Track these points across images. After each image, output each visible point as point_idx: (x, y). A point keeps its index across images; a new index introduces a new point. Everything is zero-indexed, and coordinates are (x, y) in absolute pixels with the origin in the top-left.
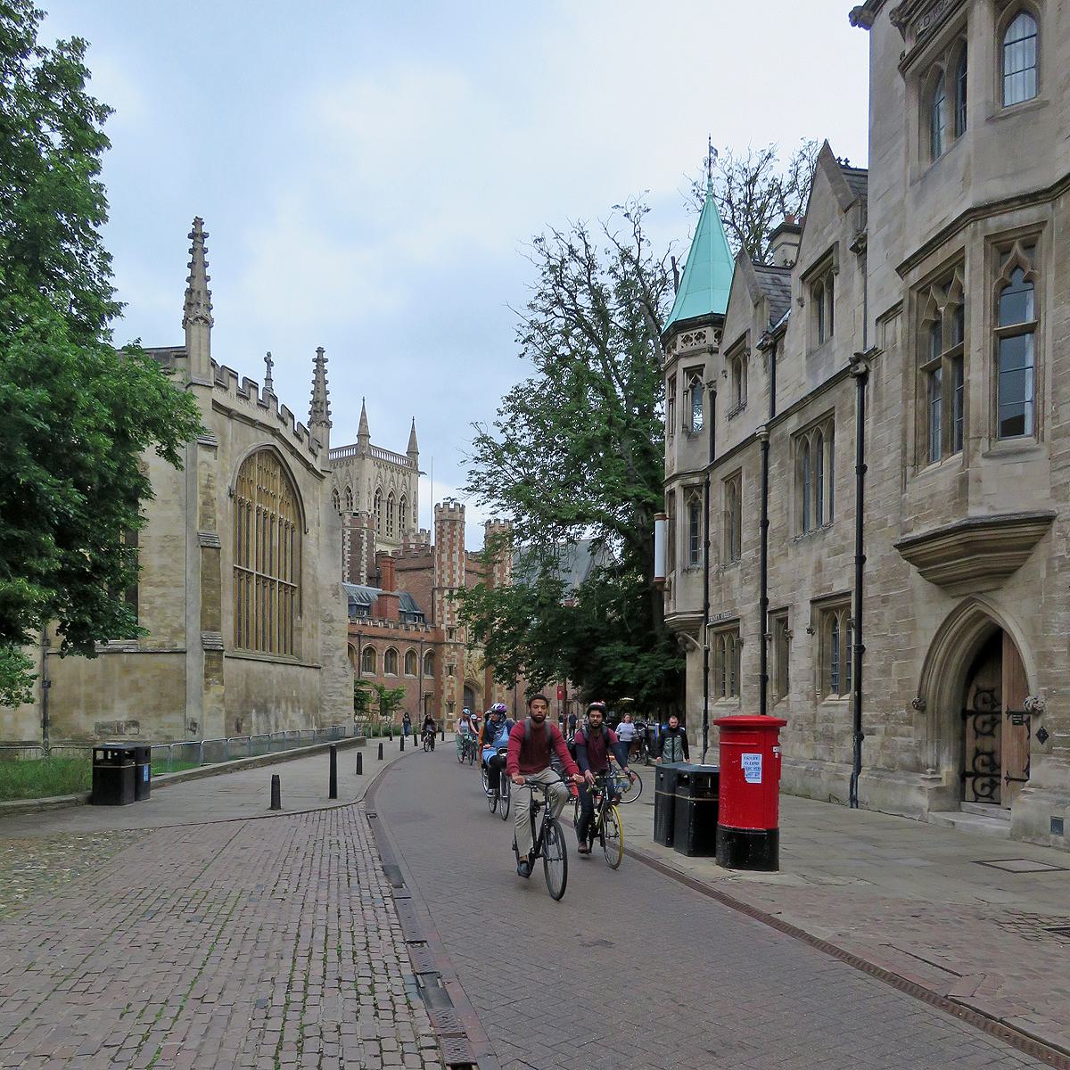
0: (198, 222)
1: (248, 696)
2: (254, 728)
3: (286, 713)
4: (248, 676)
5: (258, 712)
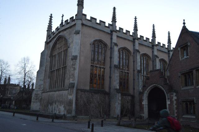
2: (49, 109)
5: (50, 105)
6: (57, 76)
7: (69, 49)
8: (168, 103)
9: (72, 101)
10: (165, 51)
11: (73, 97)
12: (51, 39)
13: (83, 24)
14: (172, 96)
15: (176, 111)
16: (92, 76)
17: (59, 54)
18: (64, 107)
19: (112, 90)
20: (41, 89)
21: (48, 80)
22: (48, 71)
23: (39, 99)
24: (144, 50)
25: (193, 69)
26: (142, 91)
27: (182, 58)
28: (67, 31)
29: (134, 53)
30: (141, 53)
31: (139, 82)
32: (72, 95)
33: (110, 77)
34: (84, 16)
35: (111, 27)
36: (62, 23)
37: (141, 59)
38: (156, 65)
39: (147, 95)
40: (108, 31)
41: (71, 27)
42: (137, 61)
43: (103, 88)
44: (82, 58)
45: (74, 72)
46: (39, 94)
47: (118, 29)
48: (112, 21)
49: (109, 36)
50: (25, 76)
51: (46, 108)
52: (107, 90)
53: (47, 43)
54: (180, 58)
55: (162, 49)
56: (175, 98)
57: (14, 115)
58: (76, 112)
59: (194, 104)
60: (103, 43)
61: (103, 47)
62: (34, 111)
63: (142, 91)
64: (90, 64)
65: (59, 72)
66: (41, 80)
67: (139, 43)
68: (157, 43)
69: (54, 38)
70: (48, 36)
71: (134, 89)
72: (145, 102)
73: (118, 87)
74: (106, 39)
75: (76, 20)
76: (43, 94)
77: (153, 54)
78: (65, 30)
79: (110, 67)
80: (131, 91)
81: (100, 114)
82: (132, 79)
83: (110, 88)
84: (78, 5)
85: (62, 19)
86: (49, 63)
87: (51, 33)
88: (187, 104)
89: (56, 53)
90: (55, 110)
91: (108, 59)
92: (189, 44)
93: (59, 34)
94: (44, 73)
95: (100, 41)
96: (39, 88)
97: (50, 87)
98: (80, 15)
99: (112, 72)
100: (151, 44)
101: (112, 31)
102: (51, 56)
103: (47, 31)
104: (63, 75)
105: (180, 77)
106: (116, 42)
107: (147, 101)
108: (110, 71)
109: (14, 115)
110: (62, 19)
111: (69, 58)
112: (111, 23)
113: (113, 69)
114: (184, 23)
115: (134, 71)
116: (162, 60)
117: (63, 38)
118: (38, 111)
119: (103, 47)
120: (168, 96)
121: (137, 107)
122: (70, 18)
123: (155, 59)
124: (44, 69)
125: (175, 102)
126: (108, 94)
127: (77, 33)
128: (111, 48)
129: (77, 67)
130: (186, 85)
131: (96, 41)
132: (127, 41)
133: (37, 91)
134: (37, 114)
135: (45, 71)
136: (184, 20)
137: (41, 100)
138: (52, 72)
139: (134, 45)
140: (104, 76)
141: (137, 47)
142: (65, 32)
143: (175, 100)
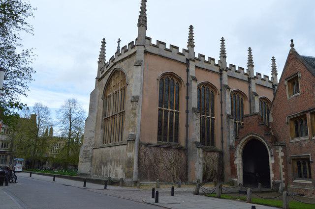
0: (104, 39)
1: (102, 160)
2: (102, 172)
3: (114, 167)
4: (102, 153)
5: (104, 166)
6: (113, 126)
7: (127, 87)
8: (272, 161)
9: (133, 159)
10: (268, 86)
11: (133, 155)
12: (103, 74)
13: (146, 52)
14: (277, 151)
15: (283, 173)
16: (162, 125)
17: (115, 94)
18: (122, 169)
19: (190, 144)
20: (92, 144)
21: (100, 131)
22: (101, 118)
23: (88, 158)
24: (235, 86)
25: (307, 112)
26: (234, 144)
27: (290, 96)
28: (125, 61)
29: (221, 90)
30: (231, 90)
31: (229, 131)
32: (132, 152)
33: (187, 126)
34: (147, 41)
35: (186, 54)
36: (118, 50)
37: (231, 98)
38: (254, 107)
39: (241, 150)
40: (183, 59)
41: (130, 56)
42: (225, 101)
43: (177, 140)
44: (146, 99)
45: (135, 120)
46: (89, 151)
47: (197, 56)
48: (188, 46)
49: (184, 68)
50: (71, 126)
51: (99, 170)
52: (182, 143)
53: (99, 79)
54: (288, 96)
55: (264, 83)
56: (281, 154)
57: (54, 180)
58: (139, 176)
59: (309, 163)
60: (175, 77)
61: (176, 82)
62: (82, 174)
63: (234, 144)
64: (158, 108)
65: (116, 119)
66: (91, 131)
67: (228, 76)
68: (255, 75)
69: (107, 72)
70: (101, 70)
71: (222, 142)
72: (238, 162)
73: (199, 140)
74: (180, 71)
75: (136, 47)
76: (95, 150)
77: (250, 90)
78: (122, 60)
79: (187, 112)
80: (218, 145)
81: (174, 178)
82: (220, 127)
83: (187, 141)
84: (139, 25)
85: (119, 45)
86: (102, 107)
87: (104, 64)
88: (299, 163)
89: (110, 93)
90: (110, 172)
91: (183, 100)
92: (300, 75)
93: (115, 67)
94: (95, 122)
95: (172, 74)
96: (89, 143)
97: (104, 141)
98: (143, 39)
99: (189, 118)
100: (247, 77)
101: (188, 60)
102: (105, 97)
103: (99, 62)
104: (121, 123)
105: (288, 123)
106: (194, 75)
107: (241, 159)
108: (187, 117)
109: (54, 180)
110: (119, 45)
111: (128, 99)
112: (187, 49)
113: (190, 113)
114: (292, 45)
115: (222, 115)
116: (264, 100)
117: (119, 72)
118: (87, 174)
119: (176, 82)
120: (271, 152)
121: (228, 169)
122: (129, 44)
123: (253, 98)
124: (95, 115)
125: (281, 161)
126: (185, 150)
127: (138, 64)
128: (188, 84)
129: (139, 111)
130: (297, 136)
131: (166, 75)
132: (210, 73)
133: (87, 146)
134: (86, 179)
135: (97, 118)
136: (292, 41)
137: (91, 159)
138: (106, 120)
139: (221, 79)
140: (178, 124)
141: (226, 81)
142: (122, 64)
143: (282, 157)
